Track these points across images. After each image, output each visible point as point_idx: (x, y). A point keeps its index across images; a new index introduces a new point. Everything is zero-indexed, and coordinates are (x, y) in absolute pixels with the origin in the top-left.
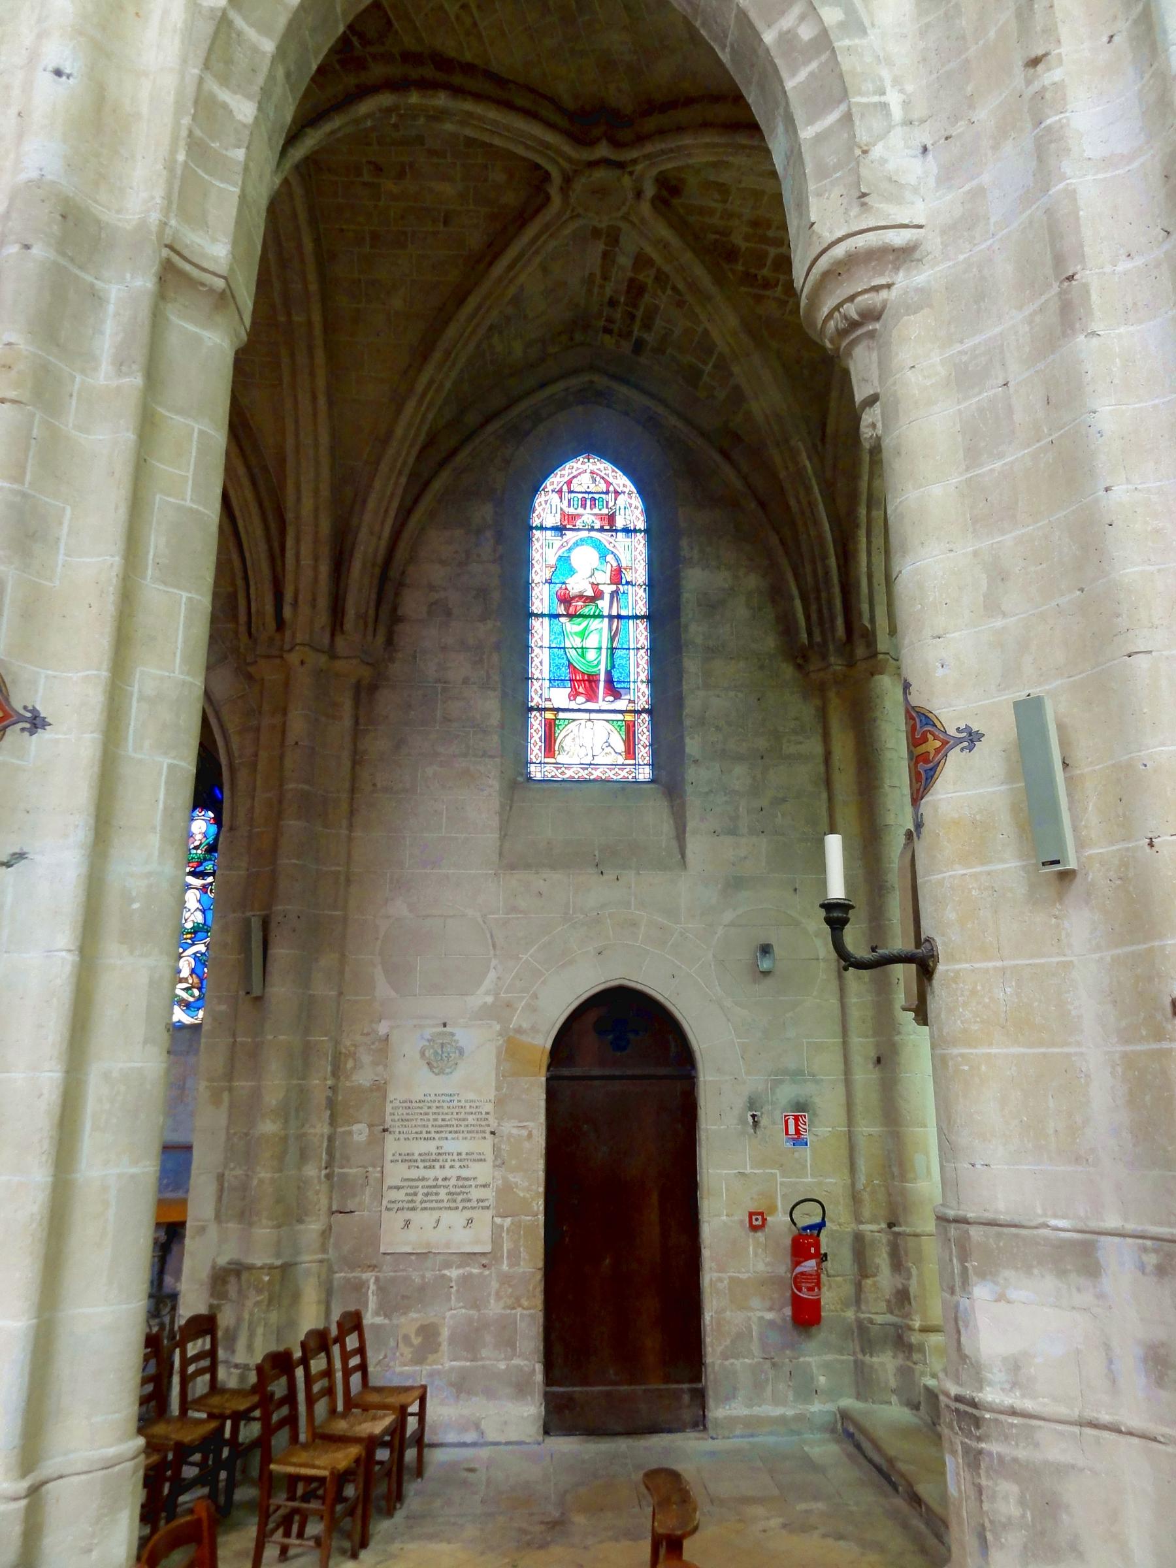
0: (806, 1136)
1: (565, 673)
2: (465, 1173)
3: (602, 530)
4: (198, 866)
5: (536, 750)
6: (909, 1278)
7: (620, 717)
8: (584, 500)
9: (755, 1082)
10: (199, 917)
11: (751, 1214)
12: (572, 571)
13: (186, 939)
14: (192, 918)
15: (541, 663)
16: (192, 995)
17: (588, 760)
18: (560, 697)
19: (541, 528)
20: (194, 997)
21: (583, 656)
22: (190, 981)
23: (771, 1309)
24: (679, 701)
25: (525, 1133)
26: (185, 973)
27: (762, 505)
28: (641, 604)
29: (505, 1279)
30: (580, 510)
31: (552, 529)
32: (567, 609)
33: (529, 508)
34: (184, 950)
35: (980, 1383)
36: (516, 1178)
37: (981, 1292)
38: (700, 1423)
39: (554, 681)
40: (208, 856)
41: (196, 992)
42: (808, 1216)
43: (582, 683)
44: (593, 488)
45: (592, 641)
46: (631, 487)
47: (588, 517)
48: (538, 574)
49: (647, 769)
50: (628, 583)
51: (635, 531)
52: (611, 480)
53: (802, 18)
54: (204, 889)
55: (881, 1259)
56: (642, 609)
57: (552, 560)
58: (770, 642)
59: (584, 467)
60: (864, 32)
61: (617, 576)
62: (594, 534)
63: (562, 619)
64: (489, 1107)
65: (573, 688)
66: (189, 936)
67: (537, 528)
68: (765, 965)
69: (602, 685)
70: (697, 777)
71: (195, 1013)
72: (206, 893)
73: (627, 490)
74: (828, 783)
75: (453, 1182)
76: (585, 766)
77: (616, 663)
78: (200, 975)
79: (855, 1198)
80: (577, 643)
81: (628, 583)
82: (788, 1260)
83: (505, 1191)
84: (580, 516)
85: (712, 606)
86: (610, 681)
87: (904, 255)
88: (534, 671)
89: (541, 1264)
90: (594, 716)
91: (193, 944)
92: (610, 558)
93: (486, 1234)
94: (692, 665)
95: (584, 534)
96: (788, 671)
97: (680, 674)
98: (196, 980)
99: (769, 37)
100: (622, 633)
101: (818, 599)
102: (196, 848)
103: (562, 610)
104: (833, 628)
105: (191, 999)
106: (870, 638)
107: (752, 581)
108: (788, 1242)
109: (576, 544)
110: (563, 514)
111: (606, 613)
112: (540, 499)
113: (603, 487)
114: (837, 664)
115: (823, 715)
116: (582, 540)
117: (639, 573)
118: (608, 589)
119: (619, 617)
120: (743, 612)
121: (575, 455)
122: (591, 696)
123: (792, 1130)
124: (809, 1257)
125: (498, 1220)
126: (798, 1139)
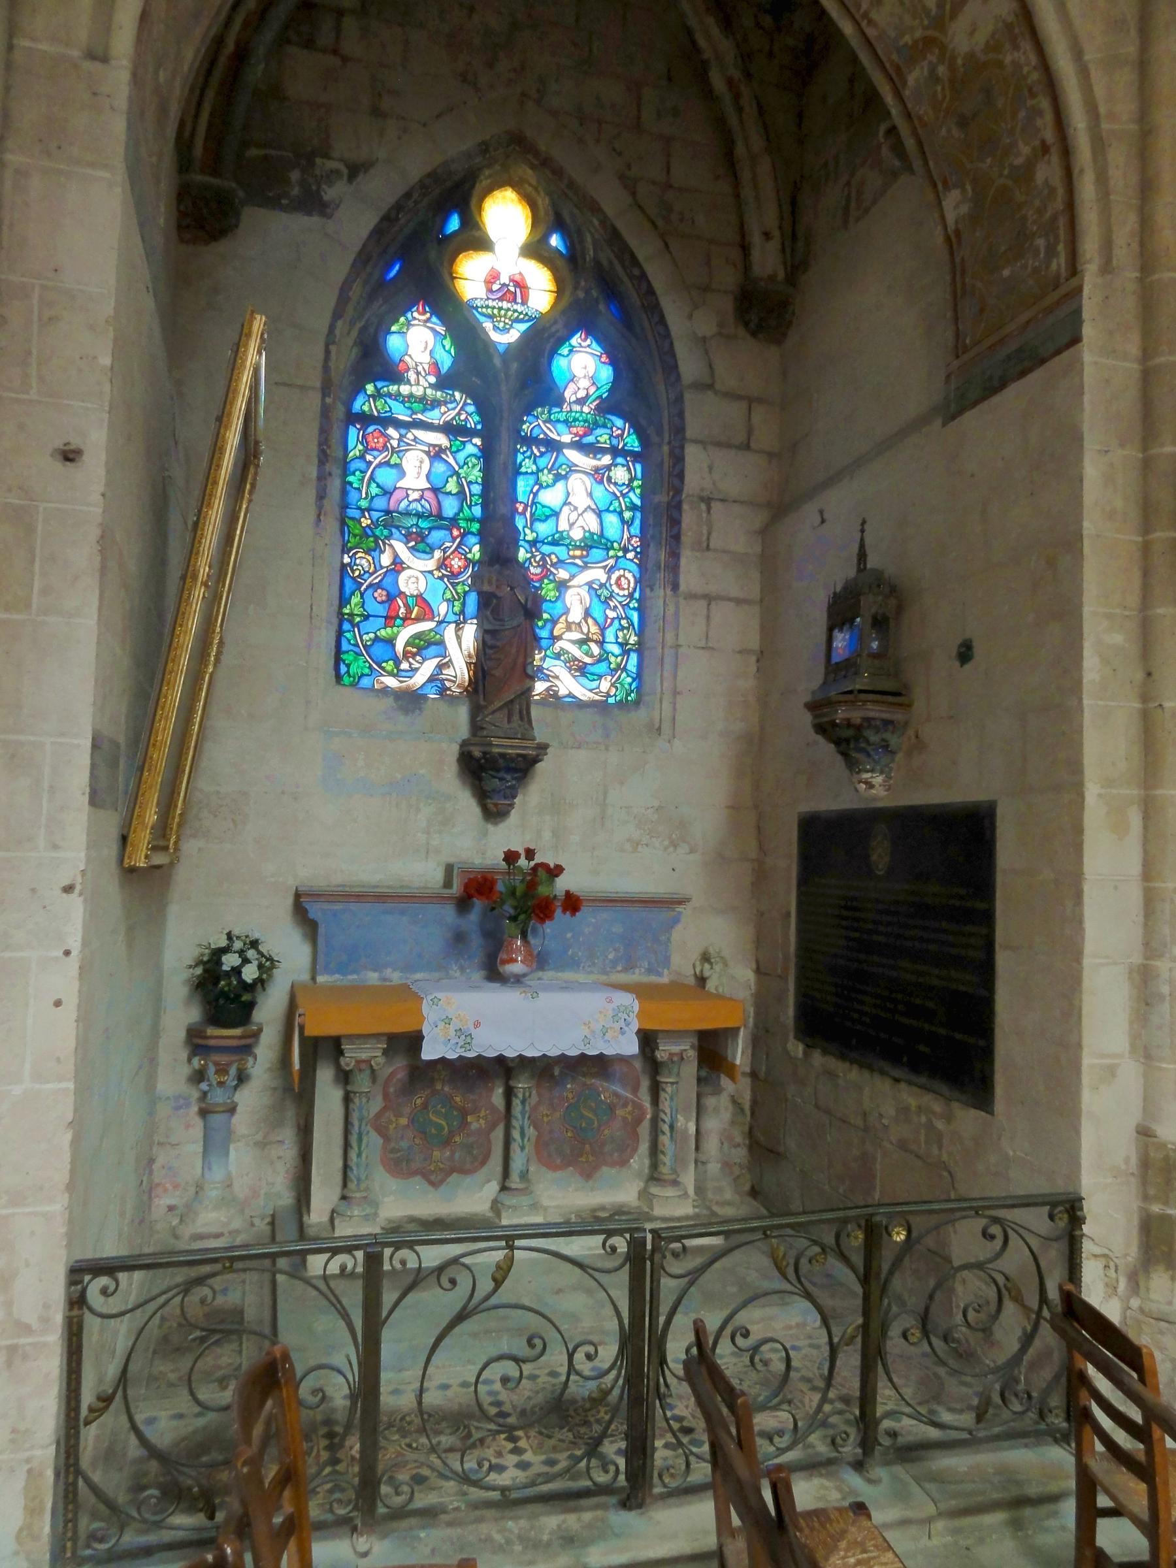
4: (585, 435)
13: (574, 557)
16: (589, 654)
20: (592, 656)
22: (585, 630)
26: (576, 615)
34: (573, 577)
40: (601, 420)
41: (596, 650)
54: (600, 475)
66: (578, 553)
71: (594, 684)
78: (601, 620)
91: (586, 567)
98: (594, 629)
102: (581, 402)
105: (588, 660)
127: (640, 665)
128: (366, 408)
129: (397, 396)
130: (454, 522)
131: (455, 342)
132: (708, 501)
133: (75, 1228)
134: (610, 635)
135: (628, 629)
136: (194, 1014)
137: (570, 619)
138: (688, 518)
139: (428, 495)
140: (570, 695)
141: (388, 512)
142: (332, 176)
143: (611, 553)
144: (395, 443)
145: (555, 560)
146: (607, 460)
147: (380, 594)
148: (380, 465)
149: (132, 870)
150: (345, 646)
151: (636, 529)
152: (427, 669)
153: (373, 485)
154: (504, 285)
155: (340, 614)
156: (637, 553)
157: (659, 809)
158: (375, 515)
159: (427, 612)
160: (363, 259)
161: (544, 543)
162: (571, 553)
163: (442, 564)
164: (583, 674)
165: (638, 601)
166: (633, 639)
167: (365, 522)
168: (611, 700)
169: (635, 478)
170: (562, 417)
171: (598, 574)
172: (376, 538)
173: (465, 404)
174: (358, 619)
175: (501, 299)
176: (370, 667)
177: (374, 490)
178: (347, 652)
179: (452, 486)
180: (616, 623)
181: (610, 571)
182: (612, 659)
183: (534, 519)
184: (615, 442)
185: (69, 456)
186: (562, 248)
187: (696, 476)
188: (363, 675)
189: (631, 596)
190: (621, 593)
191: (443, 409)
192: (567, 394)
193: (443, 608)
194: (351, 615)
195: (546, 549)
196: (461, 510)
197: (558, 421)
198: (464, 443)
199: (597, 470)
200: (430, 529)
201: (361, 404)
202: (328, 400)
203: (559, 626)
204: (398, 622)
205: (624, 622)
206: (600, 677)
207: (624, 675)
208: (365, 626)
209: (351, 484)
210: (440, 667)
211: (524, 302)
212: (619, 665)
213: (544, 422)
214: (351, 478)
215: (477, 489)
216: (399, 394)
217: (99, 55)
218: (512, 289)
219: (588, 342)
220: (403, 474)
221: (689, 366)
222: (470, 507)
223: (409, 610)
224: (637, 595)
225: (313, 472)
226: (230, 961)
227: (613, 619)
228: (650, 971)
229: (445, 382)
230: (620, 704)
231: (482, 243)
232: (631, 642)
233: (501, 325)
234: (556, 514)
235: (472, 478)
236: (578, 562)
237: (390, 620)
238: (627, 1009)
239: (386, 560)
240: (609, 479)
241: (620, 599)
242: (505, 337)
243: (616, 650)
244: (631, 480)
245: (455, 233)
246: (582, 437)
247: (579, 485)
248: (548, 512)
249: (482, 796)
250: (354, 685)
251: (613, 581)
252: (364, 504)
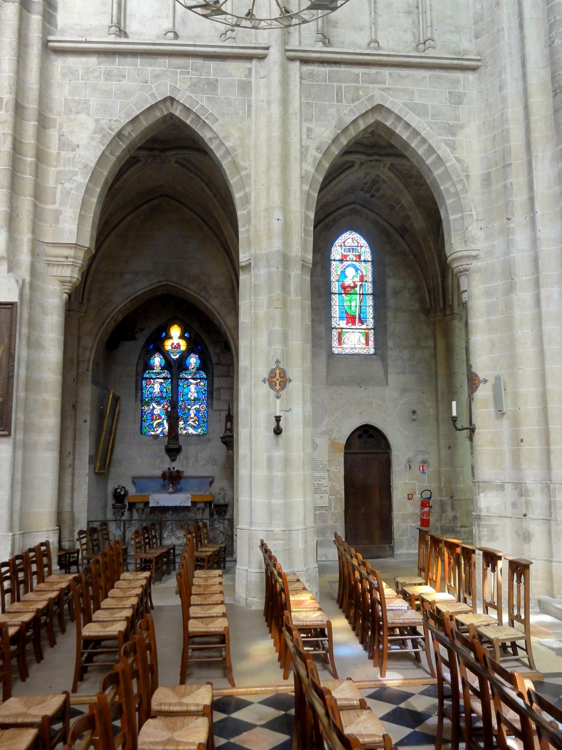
0: (425, 471)
1: (344, 315)
2: (319, 483)
3: (356, 261)
5: (335, 343)
6: (457, 512)
7: (363, 331)
8: (349, 249)
9: (410, 454)
10: (196, 395)
11: (408, 495)
12: (346, 277)
15: (336, 311)
16: (196, 424)
17: (353, 346)
18: (343, 324)
19: (335, 260)
21: (350, 309)
23: (414, 523)
24: (385, 327)
25: (338, 470)
26: (192, 415)
27: (415, 256)
28: (370, 289)
29: (333, 514)
30: (348, 253)
31: (339, 260)
32: (344, 291)
33: (330, 252)
35: (481, 511)
36: (335, 484)
37: (482, 495)
38: (392, 556)
39: (341, 318)
41: (197, 423)
42: (426, 495)
43: (351, 319)
44: (353, 245)
45: (353, 304)
46: (366, 244)
47: (351, 256)
48: (334, 278)
49: (373, 350)
50: (366, 281)
51: (368, 261)
52: (359, 241)
53: (451, 186)
54: (197, 384)
55: (449, 508)
56: (370, 291)
57: (339, 273)
58: (417, 306)
59: (349, 236)
60: (467, 192)
61: (362, 279)
62: (354, 263)
63: (343, 295)
64: (326, 462)
65: (347, 321)
67: (333, 260)
68: (414, 417)
69: (357, 319)
70: (392, 354)
73: (365, 245)
74: (435, 356)
75: (316, 485)
76: (352, 348)
77: (362, 311)
79: (440, 490)
80: (349, 304)
81: (366, 281)
82: (420, 508)
83: (332, 488)
84: (348, 255)
85: (396, 293)
86: (360, 318)
87: (475, 257)
88: (333, 315)
89: (344, 510)
90: (354, 331)
91: (194, 405)
92: (359, 272)
93: (327, 500)
94: (390, 315)
95: (350, 263)
96: (422, 316)
97: (385, 318)
99: (442, 188)
100: (364, 300)
101: (434, 292)
102: (193, 369)
103: (343, 292)
104: (439, 303)
106: (451, 307)
107: (411, 284)
108: (420, 503)
109: (347, 267)
110: (342, 255)
111: (358, 293)
112: (333, 249)
113: (356, 244)
114: (439, 315)
115: (434, 332)
116: (349, 265)
117: (369, 278)
118: (359, 284)
119: (363, 294)
120: (407, 295)
121: (346, 231)
122: (354, 323)
123: (421, 469)
124: (427, 507)
125: (330, 497)
126: (423, 472)
129: (153, 373)
130: (165, 398)
131: (165, 360)
132: (219, 389)
133: (88, 517)
134: (200, 419)
136: (113, 502)
138: (215, 393)
142: (137, 332)
146: (199, 381)
147: (150, 415)
149: (96, 473)
151: (206, 395)
152: (160, 430)
155: (142, 420)
157: (210, 457)
159: (160, 417)
160: (144, 347)
163: (163, 407)
167: (147, 400)
171: (197, 406)
177: (148, 393)
179: (165, 390)
181: (200, 406)
185: (85, 421)
187: (216, 384)
193: (163, 416)
201: (146, 376)
210: (163, 429)
215: (170, 390)
217: (88, 370)
220: (154, 389)
221: (214, 360)
225: (134, 392)
226: (119, 490)
228: (205, 492)
229: (163, 368)
230: (203, 434)
231: (171, 338)
234: (188, 394)
237: (152, 420)
238: (189, 497)
239: (151, 407)
242: (175, 357)
247: (193, 388)
249: (170, 456)
250: (145, 434)
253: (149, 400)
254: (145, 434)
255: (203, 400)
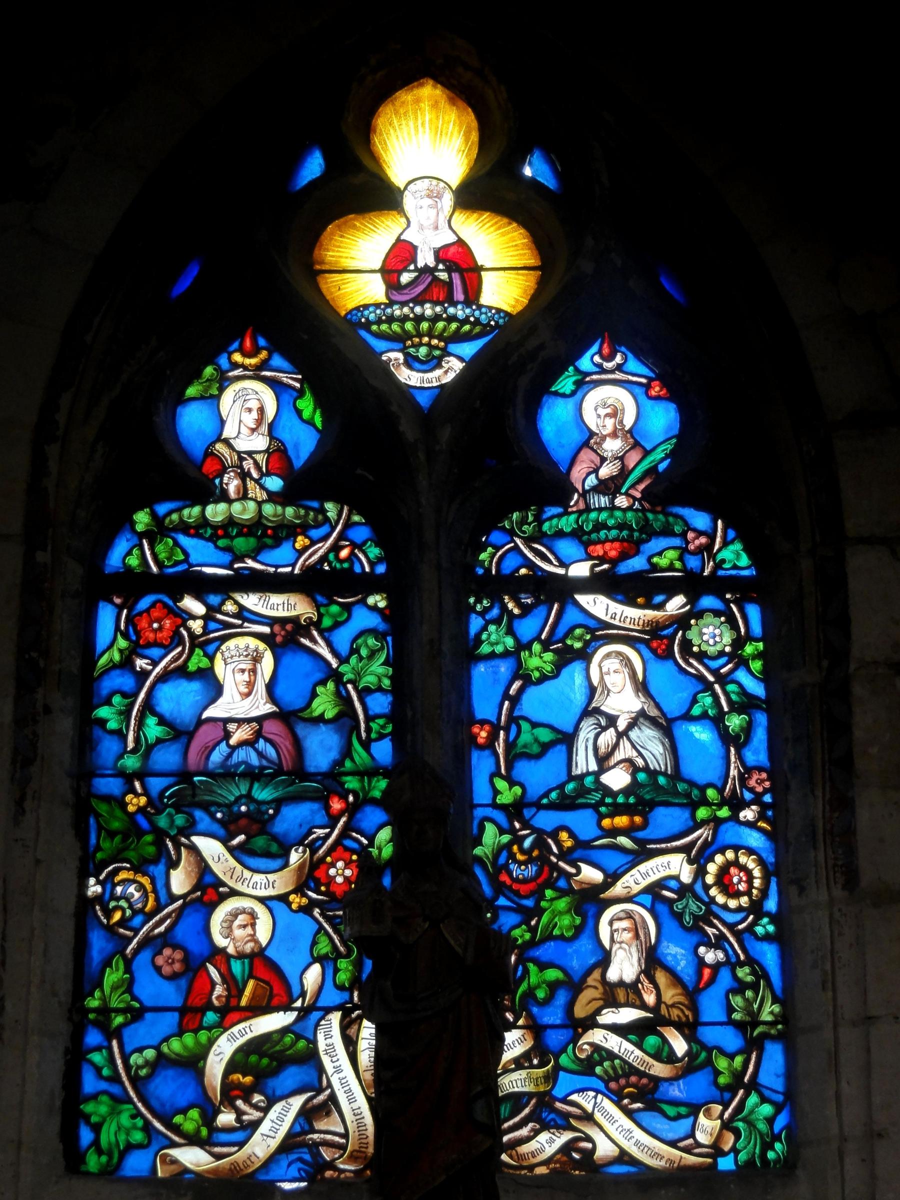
4: (624, 556)
13: (614, 832)
14: (625, 751)
16: (664, 1055)
34: (612, 878)
40: (657, 520)
66: (622, 821)
71: (684, 1125)
72: (668, 655)
91: (643, 854)
98: (670, 995)
105: (659, 1069)
127: (790, 1074)
128: (133, 561)
129: (198, 529)
135: (755, 987)
137: (613, 975)
139: (273, 728)
140: (624, 1157)
141: (184, 775)
143: (702, 813)
144: (196, 626)
145: (569, 844)
146: (676, 604)
148: (164, 677)
150: (90, 1083)
153: (151, 721)
154: (426, 270)
156: (764, 807)
158: (156, 784)
161: (539, 806)
162: (606, 822)
164: (653, 1106)
165: (774, 919)
166: (769, 1011)
167: (134, 803)
168: (726, 1164)
169: (749, 638)
170: (567, 523)
172: (160, 835)
173: (348, 525)
174: (119, 1020)
175: (419, 300)
176: (147, 1128)
177: (153, 730)
178: (94, 1097)
180: (725, 979)
182: (722, 1063)
183: (514, 755)
184: (693, 562)
186: (548, 179)
188: (130, 1147)
189: (756, 909)
190: (733, 904)
191: (301, 542)
192: (577, 474)
194: (105, 1011)
195: (546, 820)
196: (347, 752)
197: (560, 534)
198: (347, 608)
199: (654, 630)
200: (278, 803)
202: (42, 557)
203: (587, 995)
204: (211, 1017)
205: (743, 973)
206: (694, 1109)
207: (753, 1099)
208: (137, 1034)
209: (103, 722)
210: (308, 1114)
211: (472, 296)
212: (738, 1076)
213: (528, 541)
214: (103, 712)
215: (380, 703)
216: (204, 522)
218: (444, 276)
219: (618, 359)
220: (216, 690)
222: (366, 745)
223: (234, 987)
224: (771, 905)
227: (716, 967)
230: (746, 1170)
232: (766, 1016)
233: (423, 351)
234: (567, 739)
235: (369, 680)
236: (623, 841)
240: (686, 645)
241: (731, 918)
243: (730, 1039)
244: (738, 643)
245: (313, 184)
246: (614, 562)
248: (545, 735)
251: (710, 879)
252: (131, 763)
253: (156, 804)
254: (110, 1172)
255: (736, 804)
